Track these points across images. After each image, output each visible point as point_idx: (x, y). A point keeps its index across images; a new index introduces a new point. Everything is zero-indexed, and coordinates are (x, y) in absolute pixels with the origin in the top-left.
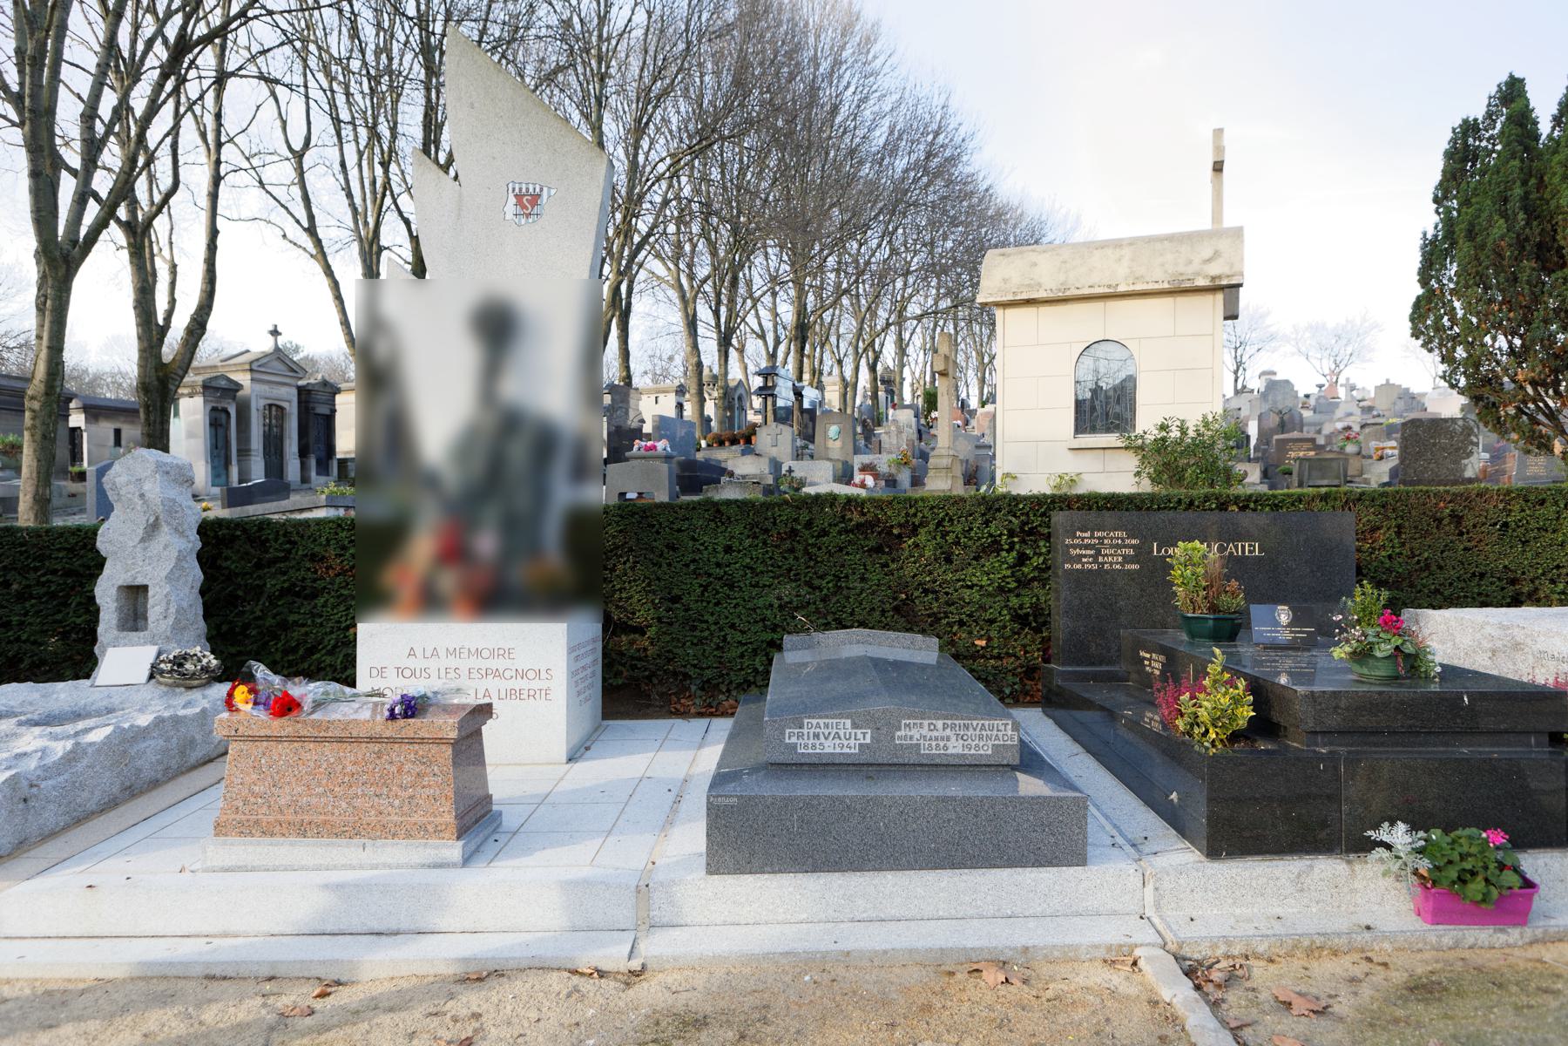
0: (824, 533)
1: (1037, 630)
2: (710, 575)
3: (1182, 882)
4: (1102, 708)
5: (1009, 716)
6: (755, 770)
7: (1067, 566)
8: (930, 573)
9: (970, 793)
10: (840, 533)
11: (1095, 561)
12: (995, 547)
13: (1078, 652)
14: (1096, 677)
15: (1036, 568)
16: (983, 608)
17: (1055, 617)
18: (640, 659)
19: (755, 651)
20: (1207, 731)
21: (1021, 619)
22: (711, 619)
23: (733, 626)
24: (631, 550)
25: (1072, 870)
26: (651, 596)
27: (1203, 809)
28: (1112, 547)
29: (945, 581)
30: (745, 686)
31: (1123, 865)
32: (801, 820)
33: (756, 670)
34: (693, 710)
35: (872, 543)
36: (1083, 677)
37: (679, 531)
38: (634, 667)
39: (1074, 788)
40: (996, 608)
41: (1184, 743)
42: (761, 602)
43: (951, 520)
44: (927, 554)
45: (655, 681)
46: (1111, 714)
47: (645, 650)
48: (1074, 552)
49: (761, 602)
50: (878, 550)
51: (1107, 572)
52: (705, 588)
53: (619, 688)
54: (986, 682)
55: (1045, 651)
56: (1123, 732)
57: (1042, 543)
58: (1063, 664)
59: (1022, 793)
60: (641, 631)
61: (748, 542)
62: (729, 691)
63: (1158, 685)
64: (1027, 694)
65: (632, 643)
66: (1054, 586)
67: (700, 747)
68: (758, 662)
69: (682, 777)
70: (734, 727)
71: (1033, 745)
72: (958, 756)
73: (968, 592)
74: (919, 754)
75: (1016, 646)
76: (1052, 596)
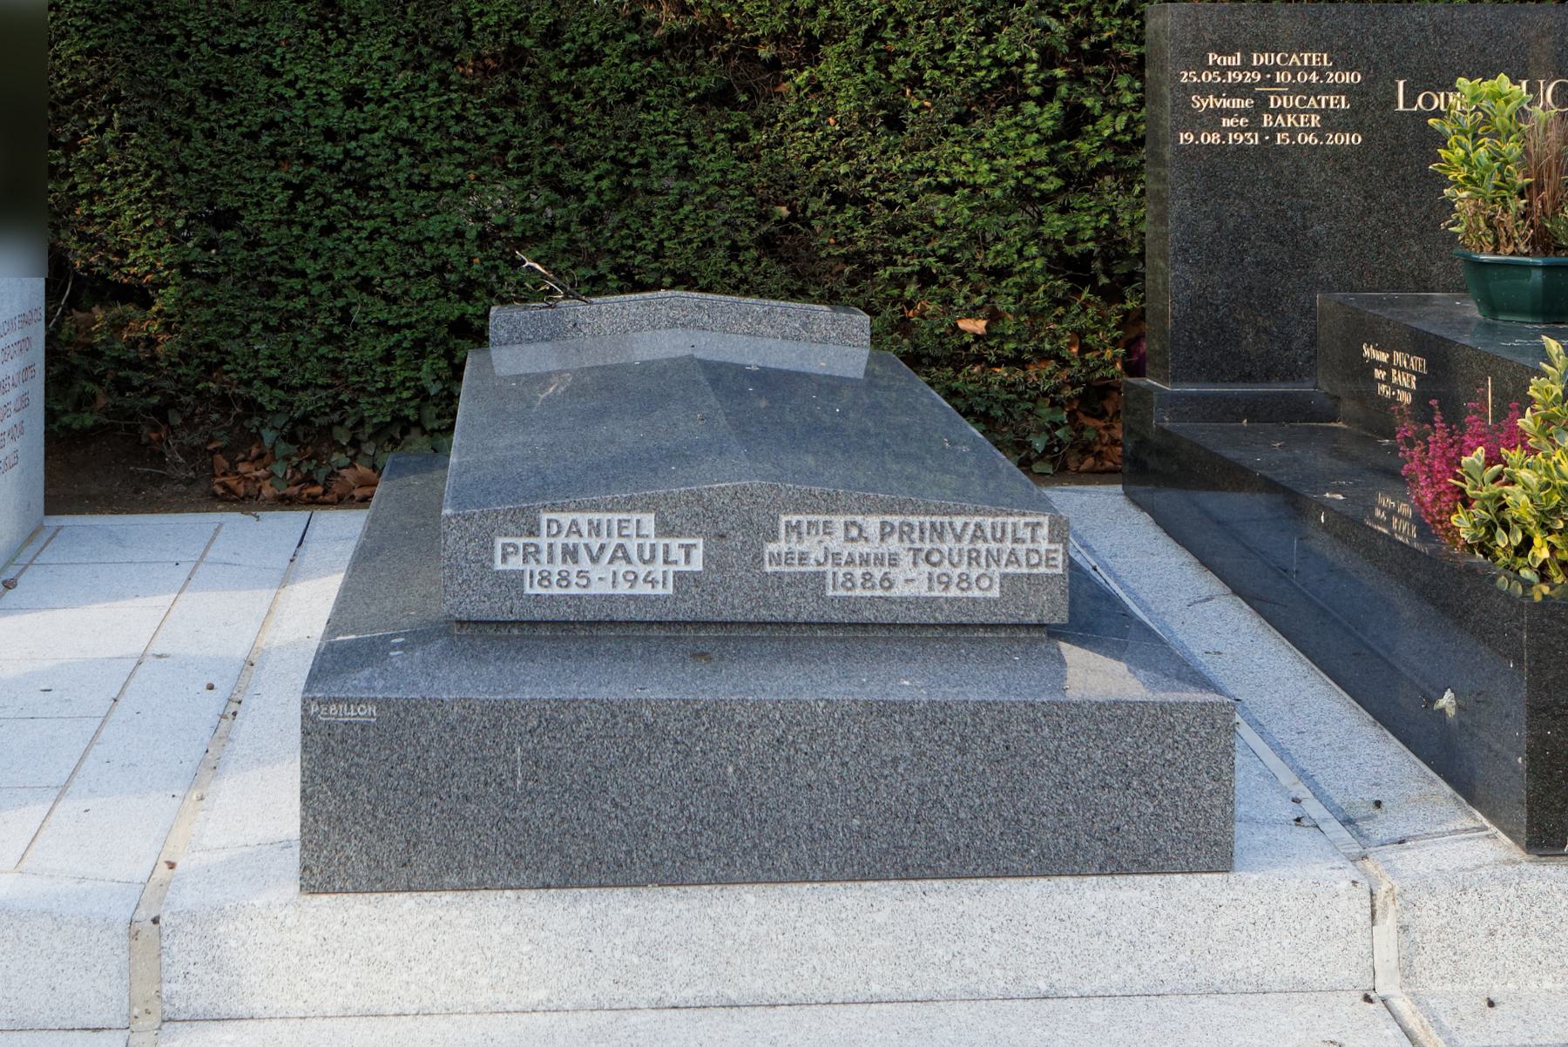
0: (590, 56)
1: (1112, 295)
2: (309, 160)
3: (1466, 910)
4: (1271, 486)
5: (1043, 505)
6: (419, 637)
7: (1186, 138)
8: (850, 154)
9: (948, 693)
10: (628, 57)
11: (1254, 125)
12: (1006, 90)
13: (1213, 348)
14: (1256, 410)
15: (1109, 142)
16: (978, 240)
17: (1155, 262)
18: (137, 366)
19: (419, 344)
20: (1528, 542)
21: (1071, 268)
22: (313, 268)
23: (365, 285)
24: (116, 98)
25: (1196, 882)
26: (165, 212)
27: (1519, 733)
28: (1294, 89)
29: (886, 175)
30: (396, 431)
31: (1320, 870)
32: (533, 757)
33: (422, 393)
34: (267, 491)
35: (706, 82)
36: (1225, 410)
37: (234, 50)
38: (122, 386)
39: (1203, 681)
40: (1017, 245)
41: (1471, 570)
42: (434, 227)
43: (900, 25)
44: (842, 107)
45: (176, 420)
46: (1293, 501)
47: (151, 342)
48: (1201, 103)
49: (434, 227)
50: (722, 97)
51: (1283, 152)
52: (298, 191)
53: (85, 436)
54: (986, 421)
55: (1131, 345)
56: (1321, 543)
57: (1122, 82)
58: (1175, 379)
59: (1073, 695)
60: (140, 296)
61: (401, 79)
62: (355, 443)
63: (1408, 428)
64: (1086, 450)
65: (118, 326)
66: (1152, 186)
67: (286, 579)
68: (428, 373)
69: (240, 651)
70: (368, 532)
71: (1102, 577)
72: (917, 602)
73: (943, 200)
74: (821, 597)
75: (1059, 333)
76: (1149, 209)
